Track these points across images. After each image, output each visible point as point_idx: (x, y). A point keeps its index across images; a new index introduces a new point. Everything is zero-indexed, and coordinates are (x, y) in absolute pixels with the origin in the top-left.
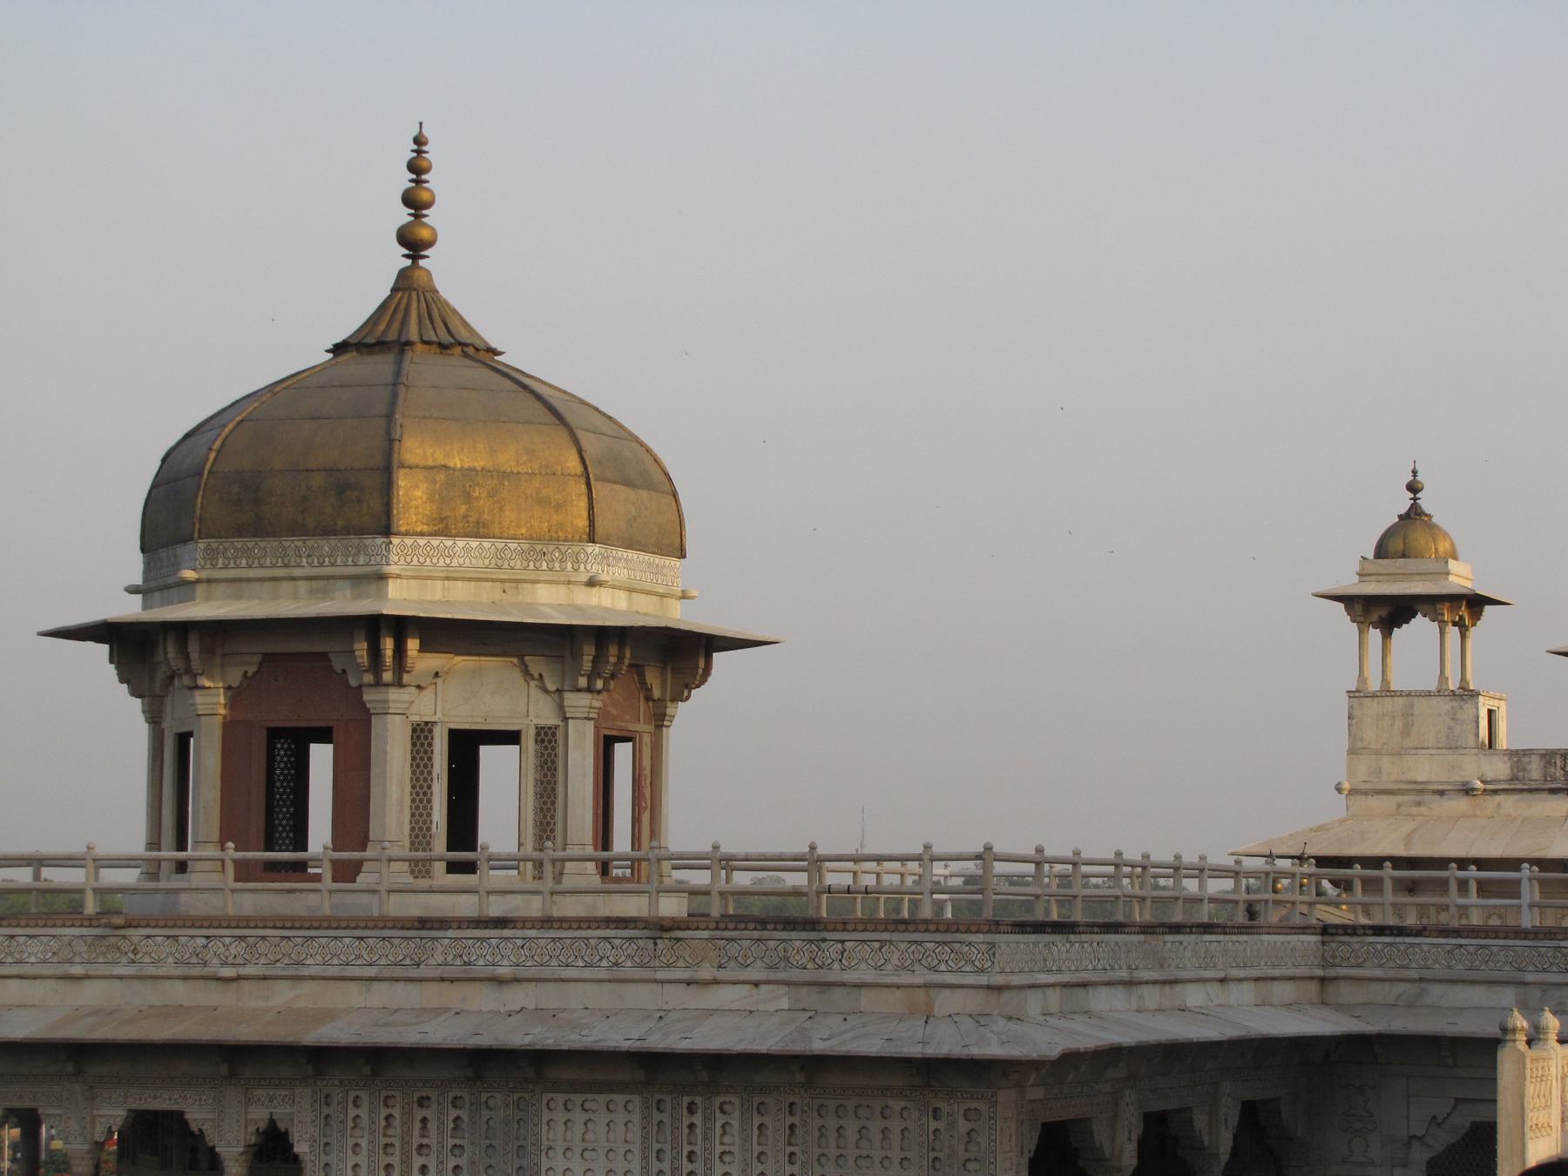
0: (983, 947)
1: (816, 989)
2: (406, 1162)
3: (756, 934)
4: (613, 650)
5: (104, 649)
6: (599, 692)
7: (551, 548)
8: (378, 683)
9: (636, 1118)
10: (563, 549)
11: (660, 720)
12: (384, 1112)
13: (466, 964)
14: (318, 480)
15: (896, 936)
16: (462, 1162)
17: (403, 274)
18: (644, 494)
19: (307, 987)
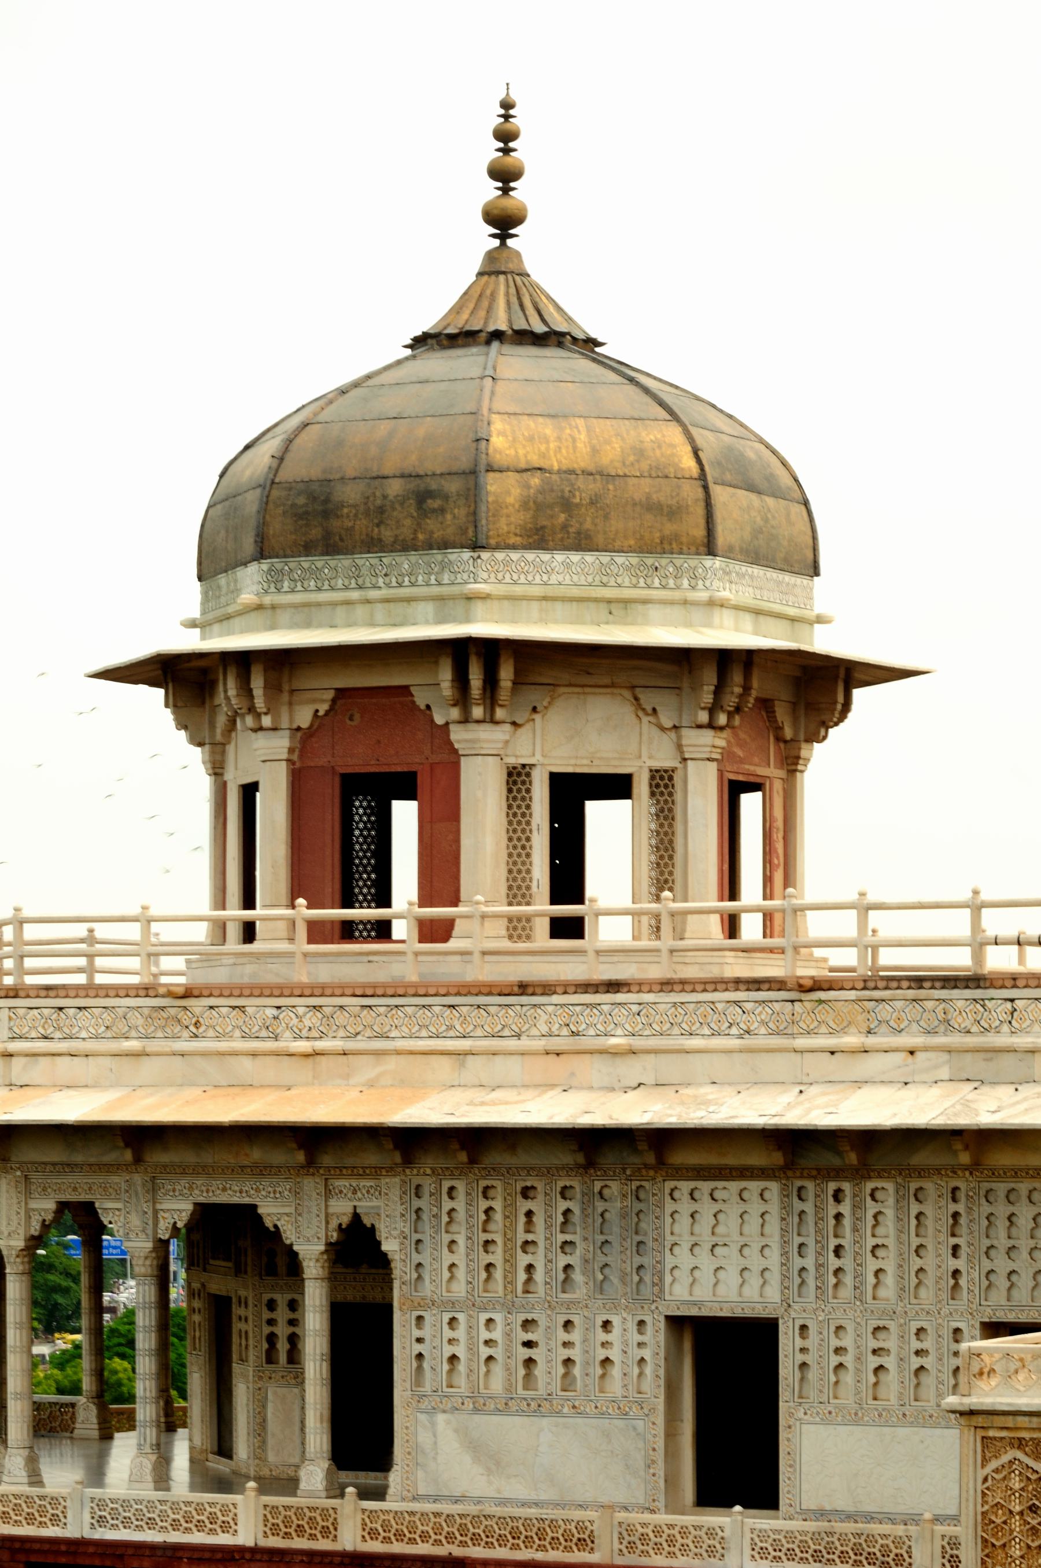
1: (982, 1055)
3: (911, 993)
4: (737, 677)
5: (160, 692)
6: (721, 729)
7: (664, 562)
8: (466, 719)
9: (774, 1207)
10: (678, 562)
11: (792, 764)
12: (484, 1204)
14: (395, 488)
16: (574, 1260)
17: (491, 256)
18: (770, 501)
19: (391, 1063)
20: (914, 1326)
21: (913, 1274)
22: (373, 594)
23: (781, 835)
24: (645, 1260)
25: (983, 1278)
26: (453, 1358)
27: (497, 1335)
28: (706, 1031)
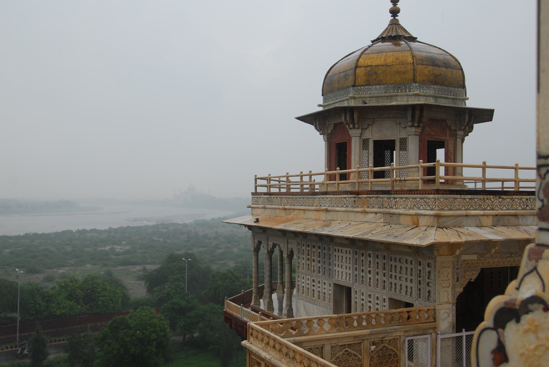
0: (433, 200)
1: (389, 215)
2: (311, 263)
4: (417, 113)
6: (418, 126)
8: (351, 129)
9: (351, 256)
14: (342, 75)
15: (410, 196)
17: (391, 21)
20: (376, 295)
23: (452, 154)
24: (330, 267)
27: (309, 282)
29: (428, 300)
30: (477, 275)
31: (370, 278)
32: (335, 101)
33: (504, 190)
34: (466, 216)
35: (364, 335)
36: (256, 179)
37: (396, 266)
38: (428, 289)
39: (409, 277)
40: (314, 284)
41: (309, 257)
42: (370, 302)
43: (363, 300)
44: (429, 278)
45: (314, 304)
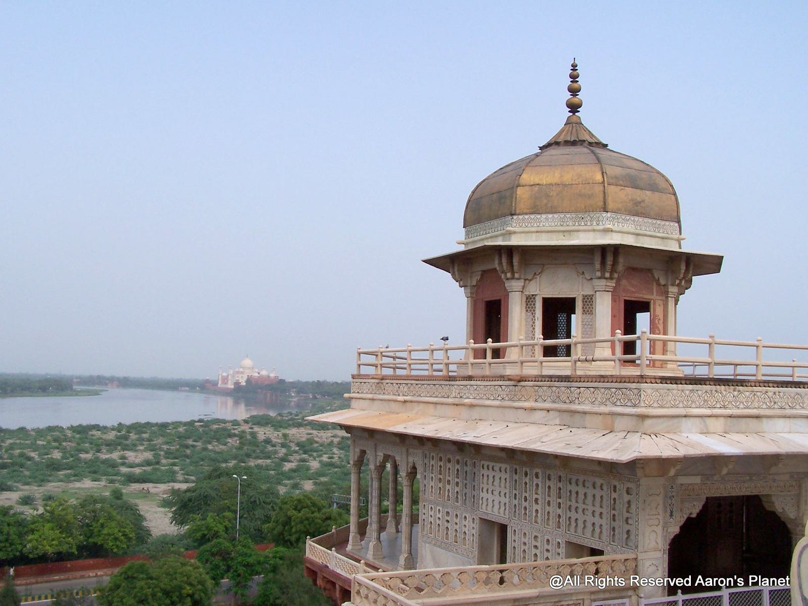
0: (636, 391)
2: (444, 487)
6: (611, 278)
7: (586, 216)
8: (508, 279)
9: (508, 476)
13: (461, 397)
18: (648, 193)
20: (546, 537)
21: (546, 513)
22: (488, 235)
24: (475, 493)
25: (567, 520)
26: (431, 522)
28: (493, 398)
29: (627, 545)
30: (701, 508)
31: (537, 511)
32: (483, 236)
33: (738, 377)
34: (685, 416)
35: (530, 598)
36: (359, 354)
37: (577, 493)
38: (627, 527)
39: (598, 510)
40: (448, 518)
41: (441, 477)
42: (536, 547)
43: (525, 544)
44: (628, 512)
45: (447, 549)
